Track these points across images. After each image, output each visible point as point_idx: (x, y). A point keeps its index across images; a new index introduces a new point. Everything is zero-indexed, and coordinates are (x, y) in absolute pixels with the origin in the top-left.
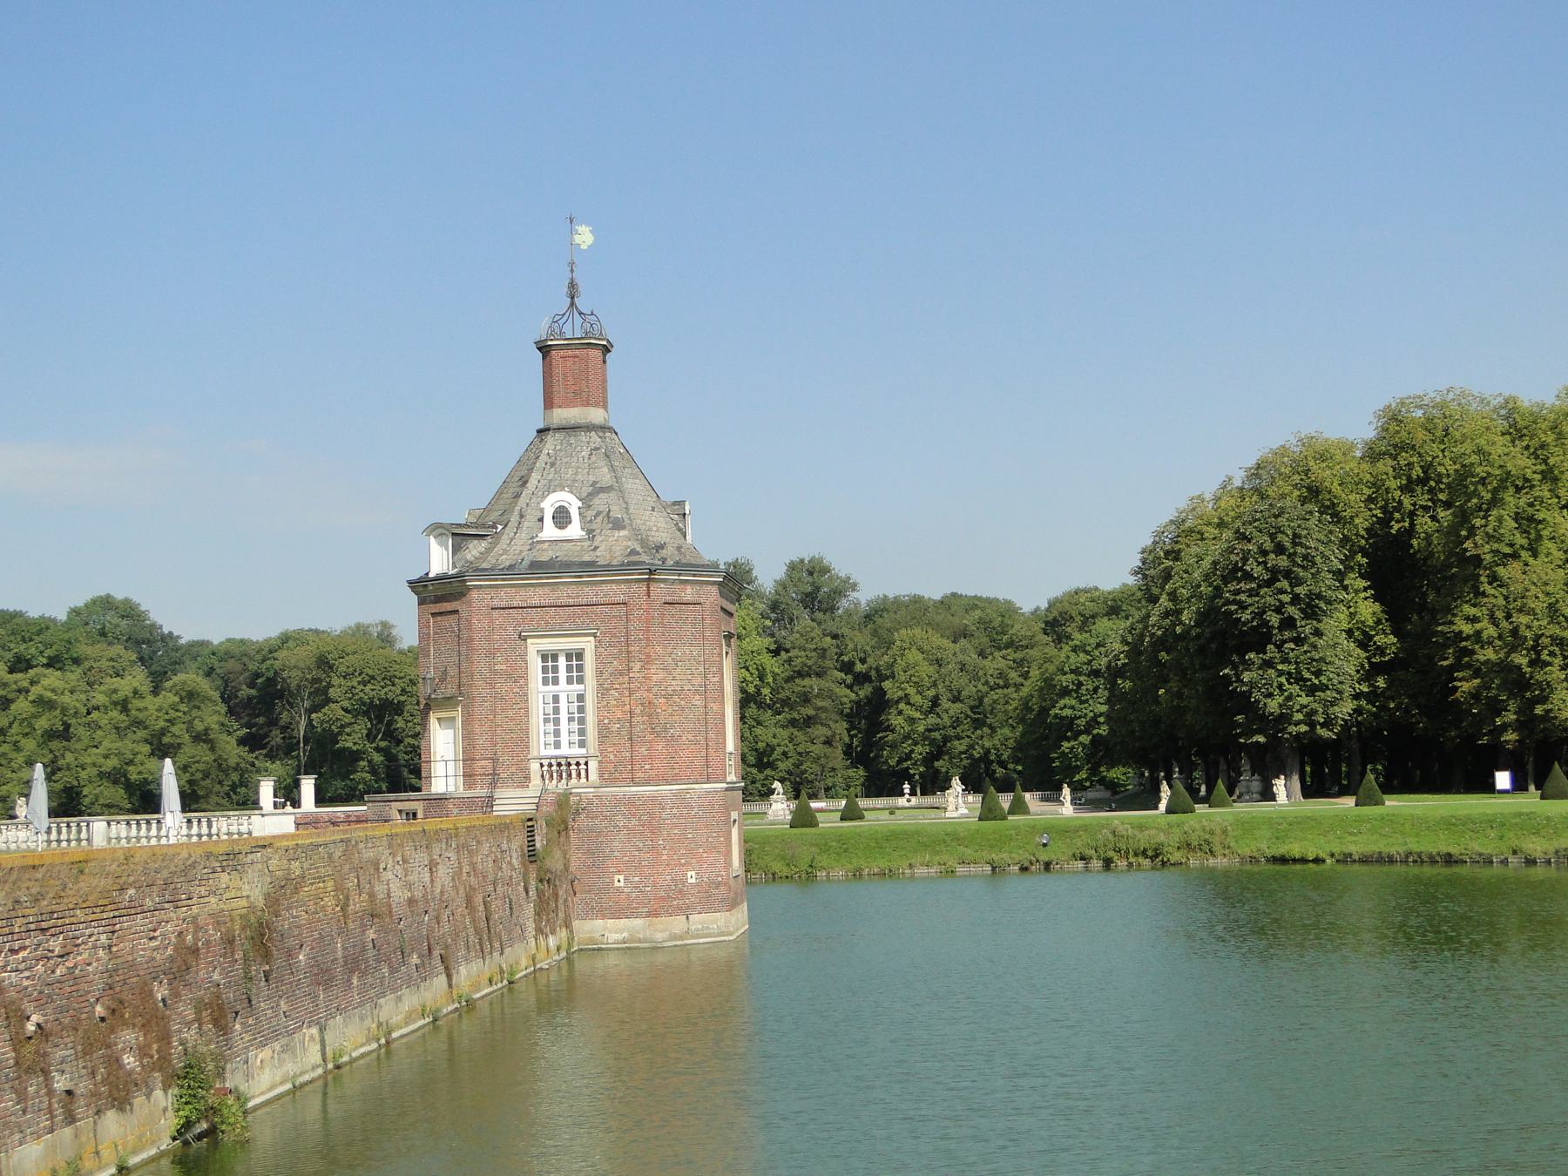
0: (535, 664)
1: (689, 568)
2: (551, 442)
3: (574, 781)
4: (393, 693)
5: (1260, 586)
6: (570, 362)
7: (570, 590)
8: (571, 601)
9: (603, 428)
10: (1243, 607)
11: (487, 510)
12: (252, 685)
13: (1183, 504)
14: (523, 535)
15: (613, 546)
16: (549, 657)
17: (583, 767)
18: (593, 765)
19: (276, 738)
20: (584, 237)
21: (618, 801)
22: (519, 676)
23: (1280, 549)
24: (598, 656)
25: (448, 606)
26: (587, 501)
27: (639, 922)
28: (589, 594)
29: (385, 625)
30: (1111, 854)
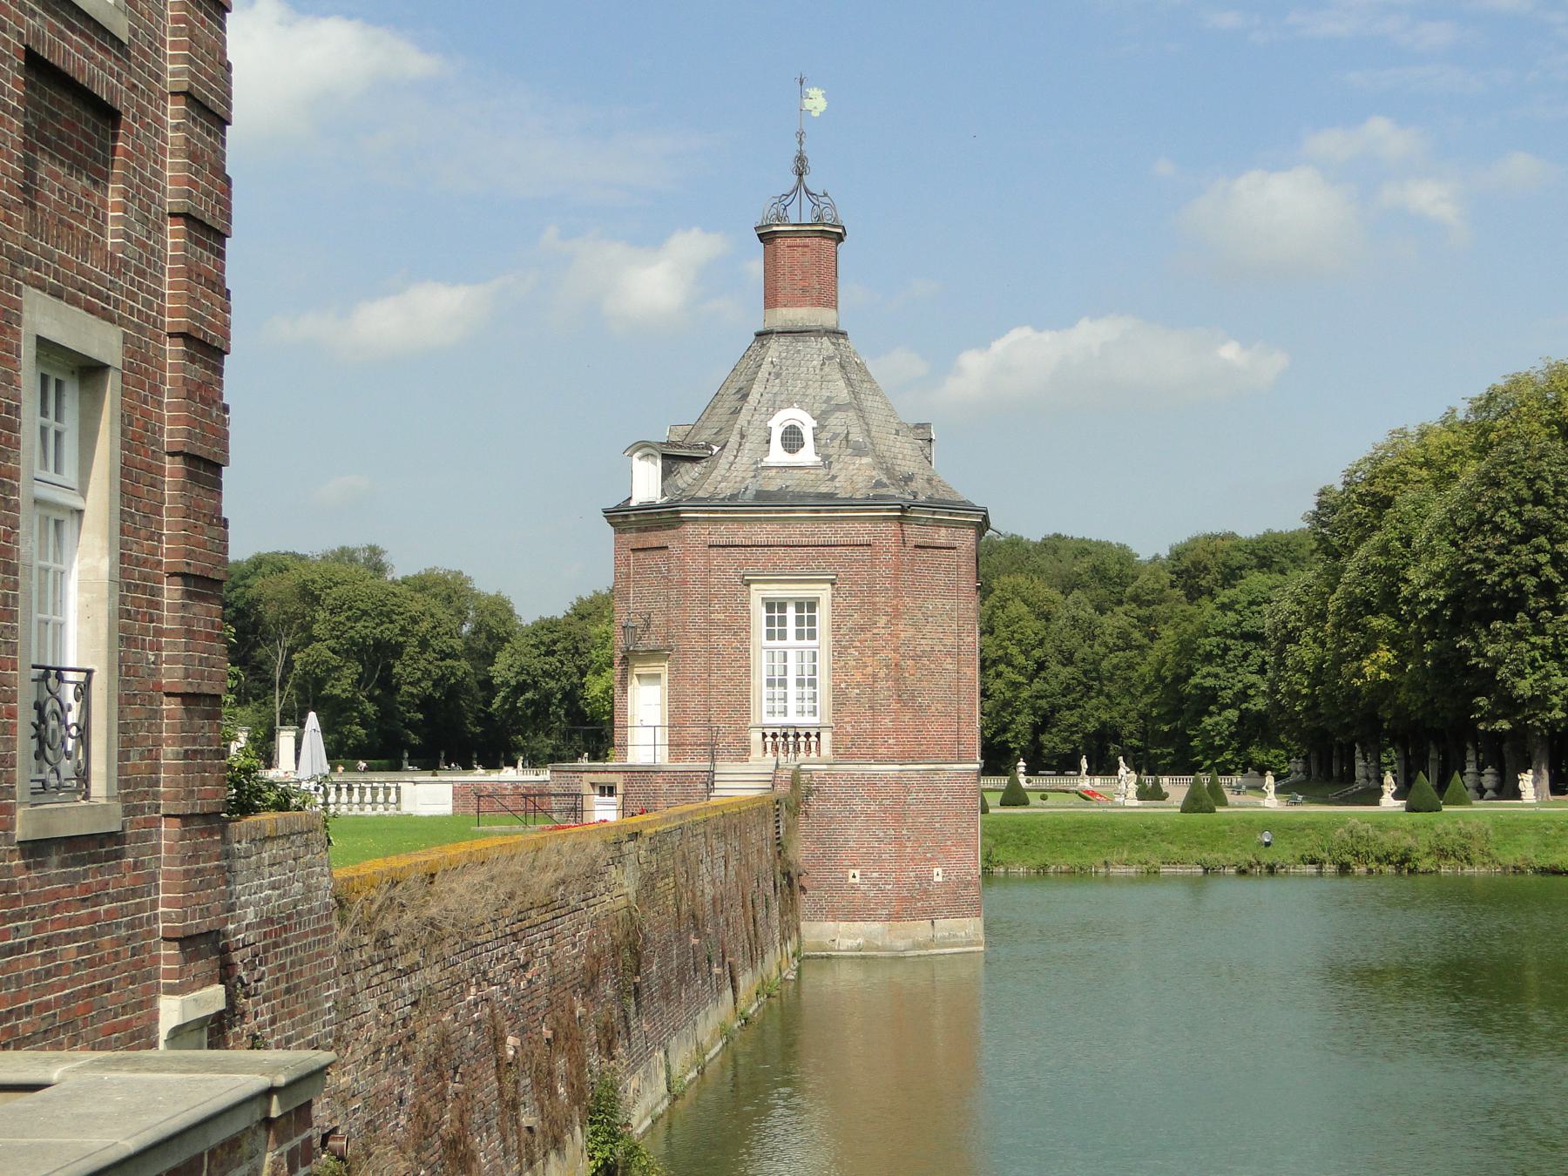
0: (759, 614)
1: (948, 510)
2: (775, 348)
3: (802, 755)
4: (390, 632)
5: (1511, 542)
7: (806, 528)
8: (805, 541)
9: (836, 334)
10: (1490, 566)
11: (697, 427)
13: (1382, 438)
14: (745, 459)
15: (855, 476)
16: (774, 606)
17: (813, 739)
18: (826, 737)
20: (816, 102)
21: (855, 782)
22: (741, 629)
23: (1539, 499)
24: (834, 606)
25: (654, 539)
26: (821, 419)
27: (877, 926)
28: (826, 533)
29: (374, 551)
30: (1348, 858)
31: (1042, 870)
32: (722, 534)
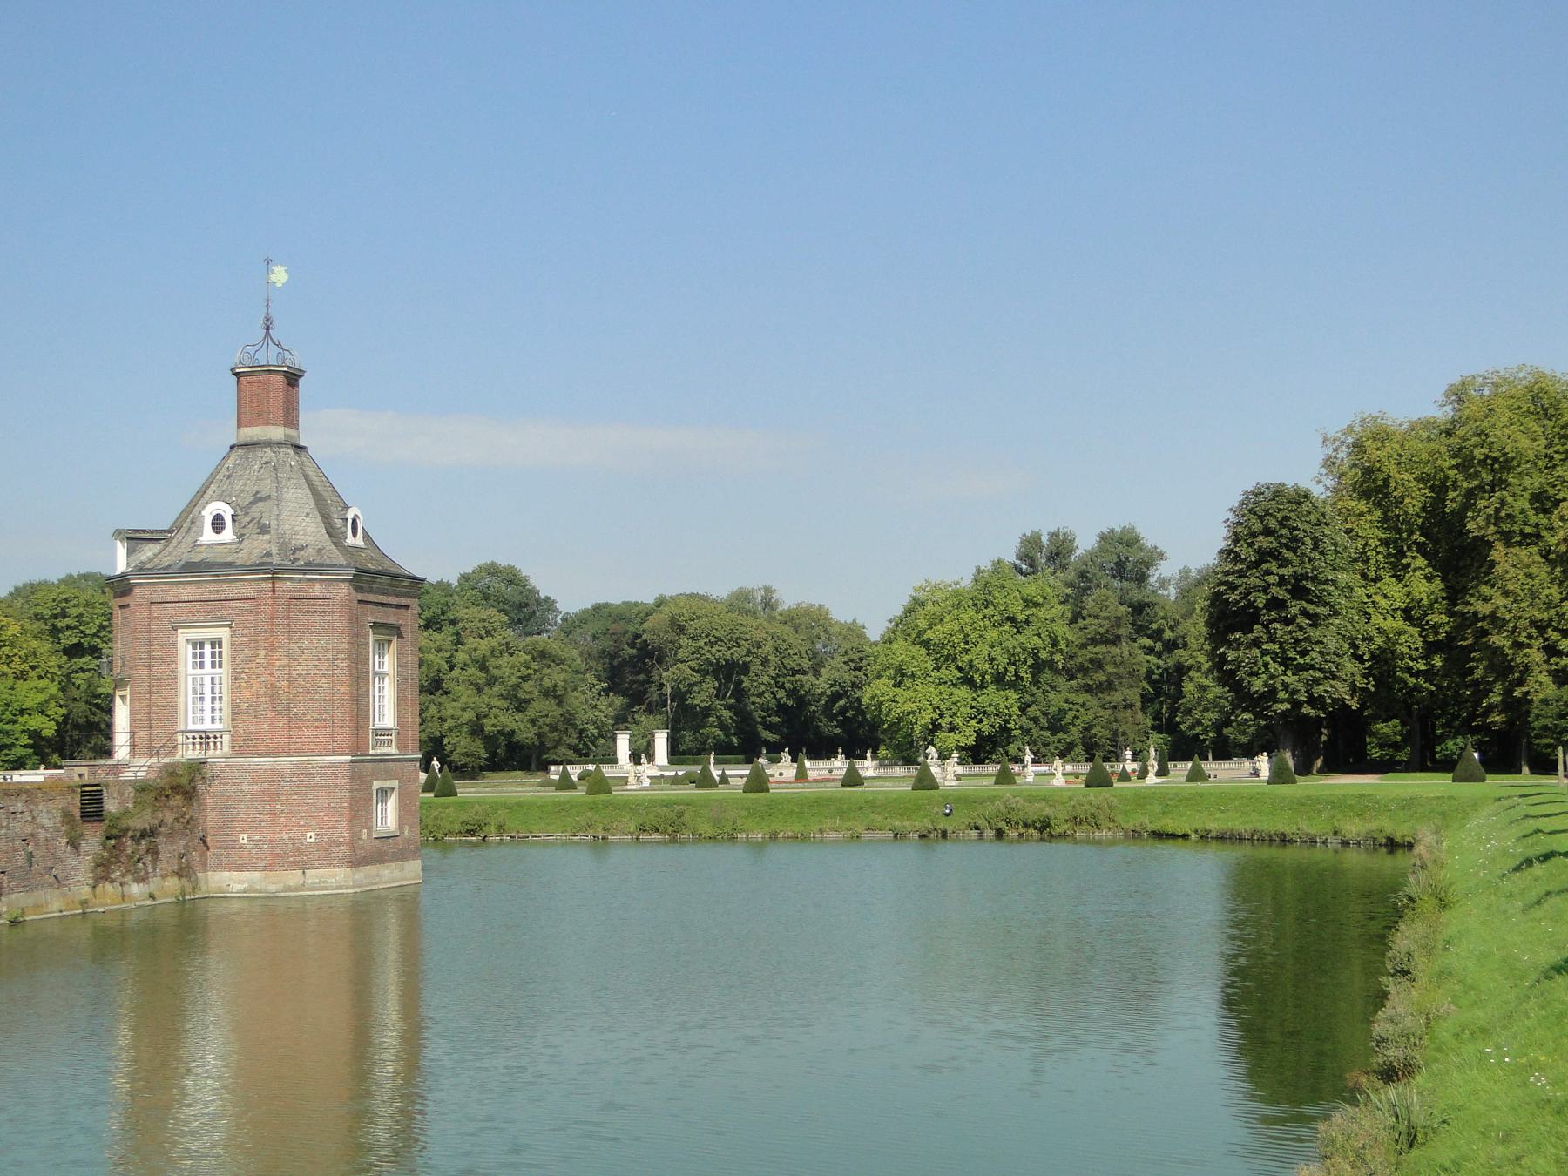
4: (738, 655)
5: (1249, 568)
6: (272, 389)
7: (213, 587)
12: (632, 645)
14: (189, 539)
15: (257, 546)
19: (654, 695)
21: (246, 770)
22: (170, 661)
23: (1268, 532)
24: (233, 644)
25: (126, 600)
27: (257, 875)
28: (227, 591)
29: (767, 589)
30: (1002, 825)
31: (773, 837)
32: (159, 593)
